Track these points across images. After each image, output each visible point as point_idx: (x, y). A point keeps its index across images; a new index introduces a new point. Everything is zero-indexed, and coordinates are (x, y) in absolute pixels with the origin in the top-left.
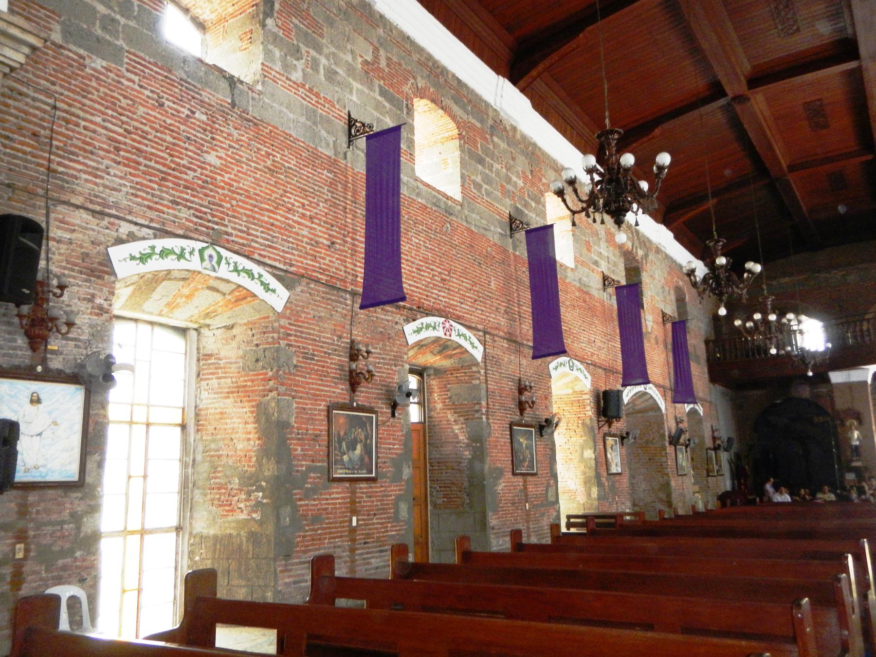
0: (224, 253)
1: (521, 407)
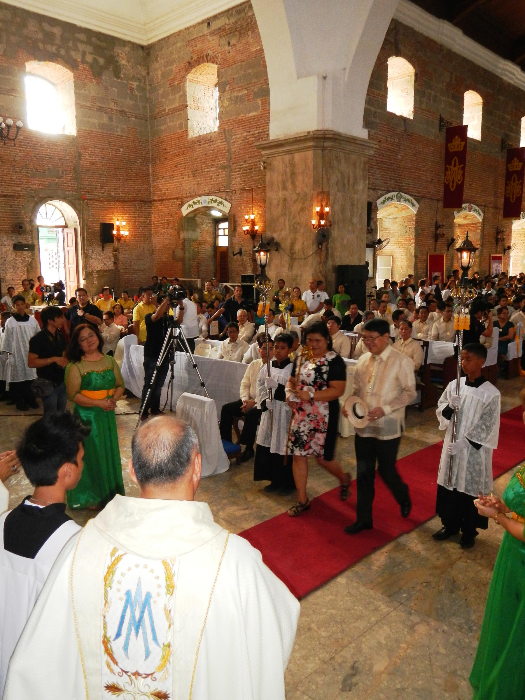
0: (402, 194)
1: (497, 240)
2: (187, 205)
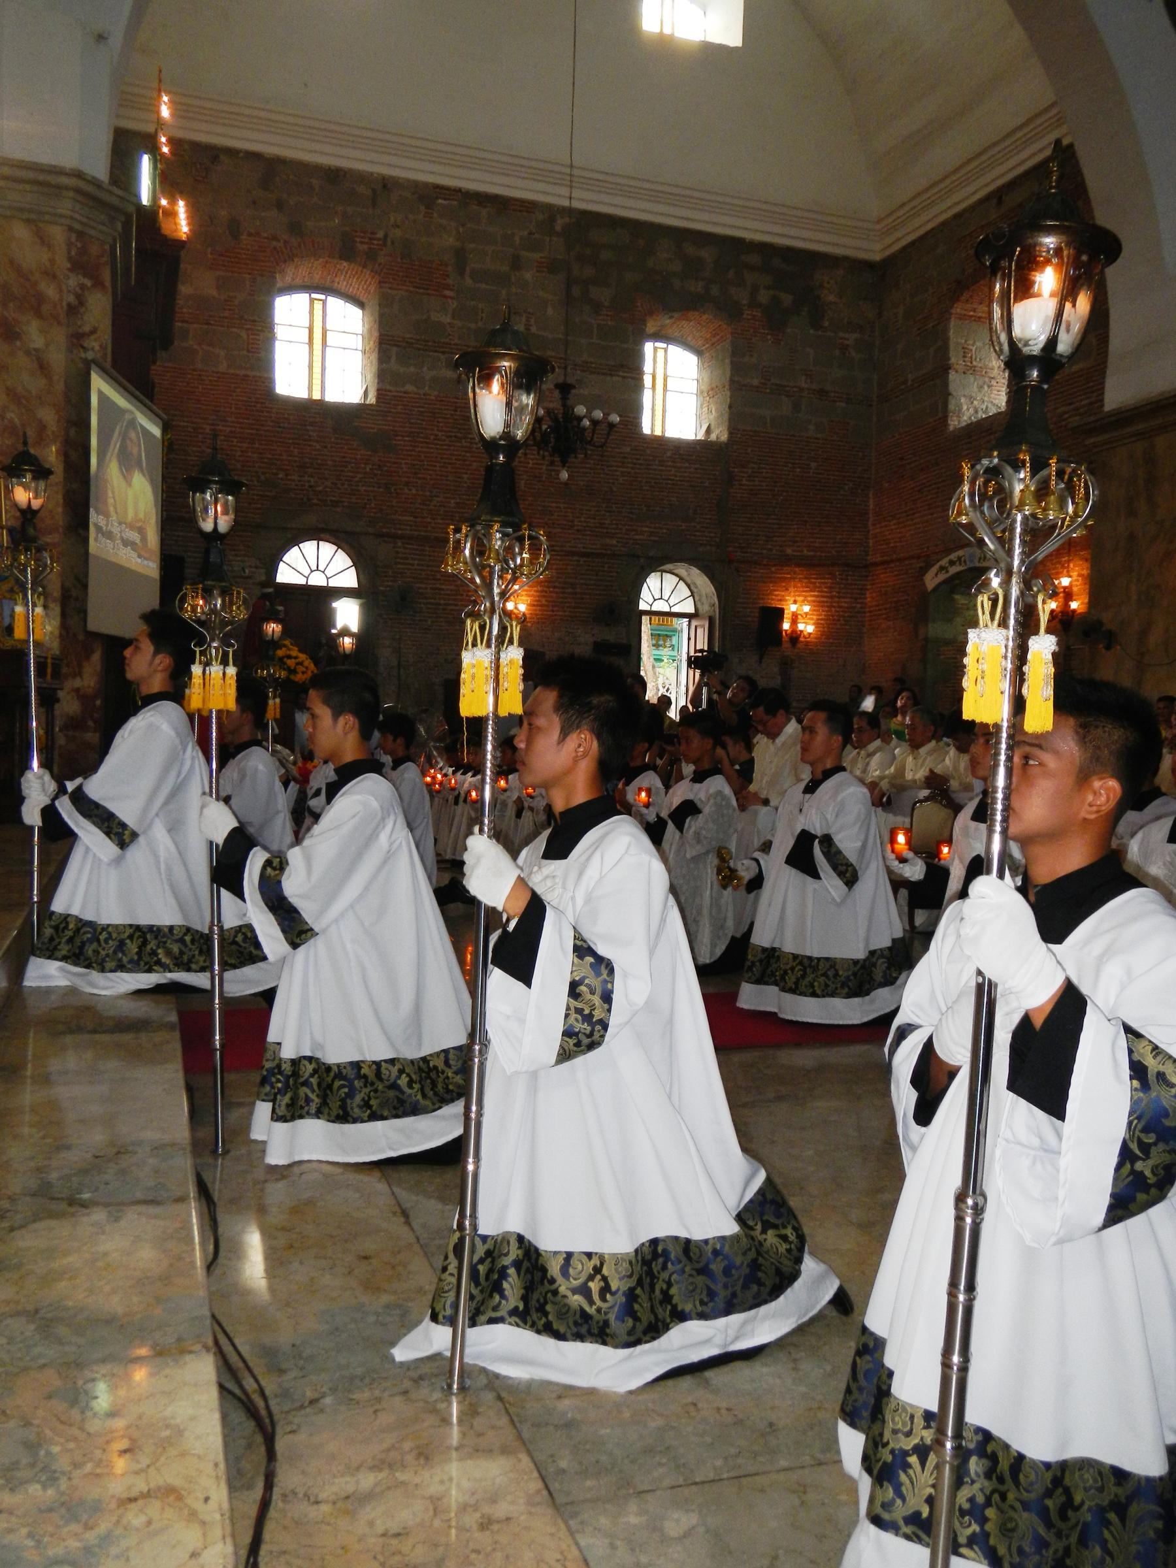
2: (937, 567)
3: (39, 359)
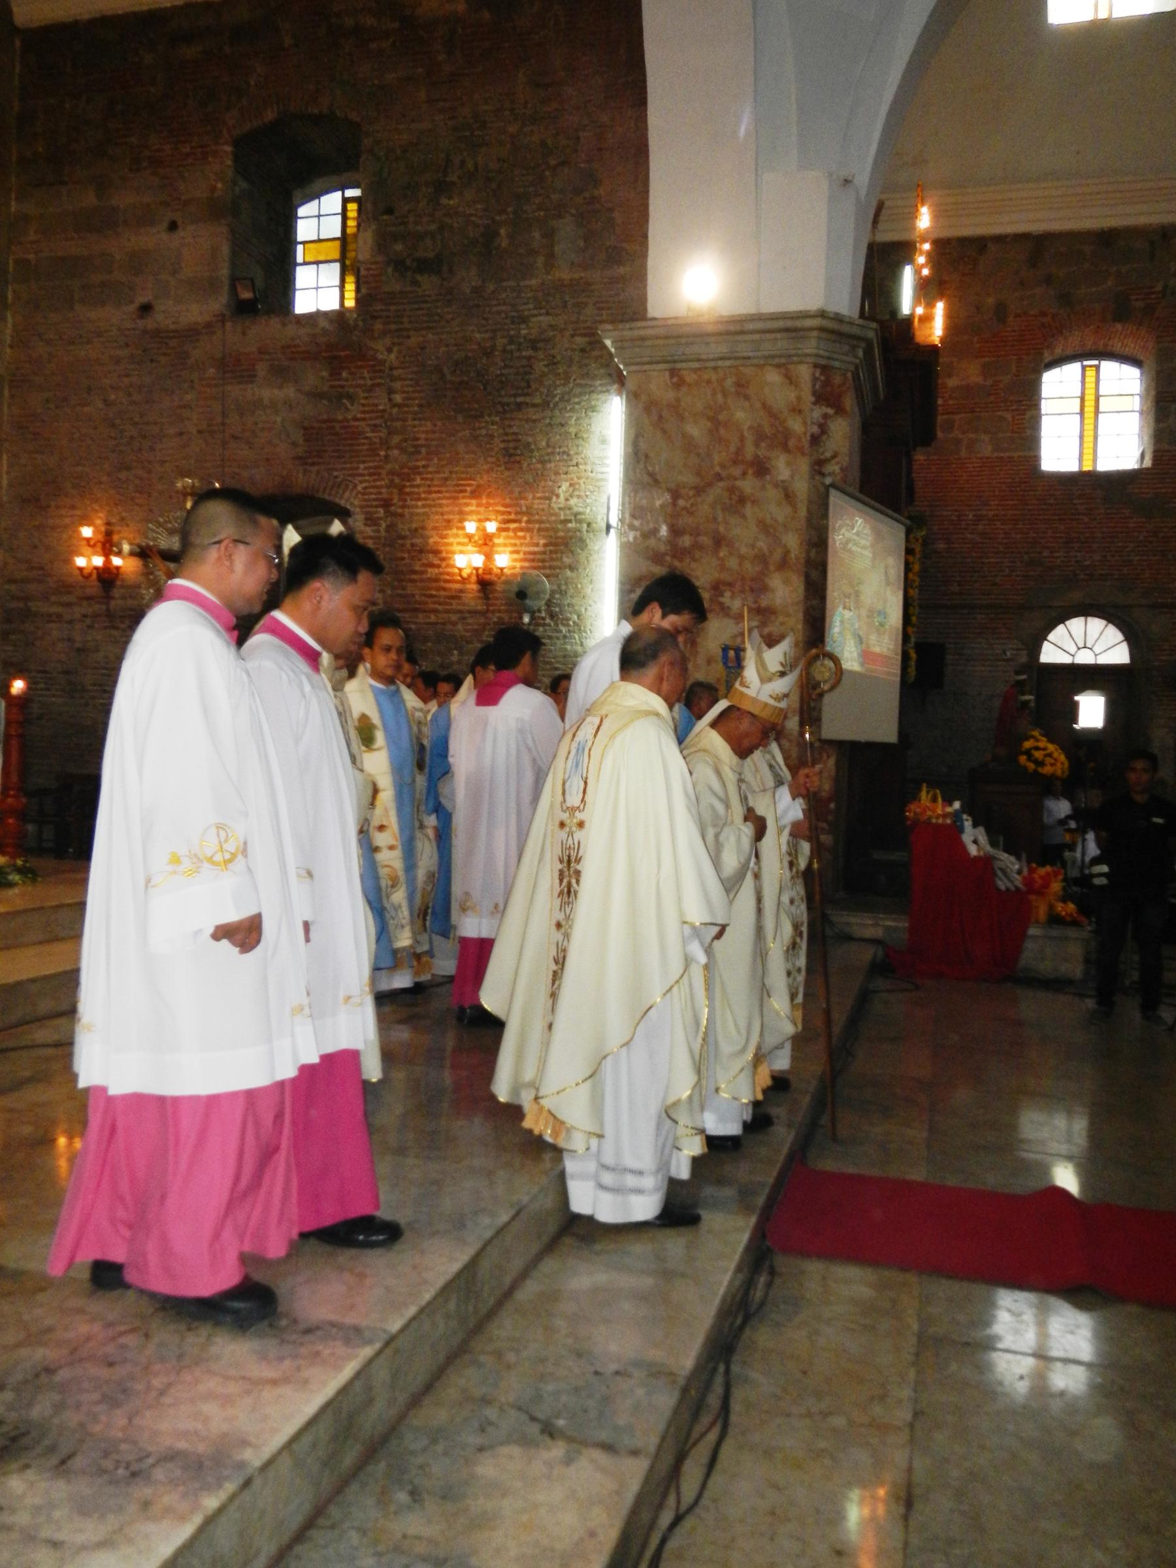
3: (785, 489)
